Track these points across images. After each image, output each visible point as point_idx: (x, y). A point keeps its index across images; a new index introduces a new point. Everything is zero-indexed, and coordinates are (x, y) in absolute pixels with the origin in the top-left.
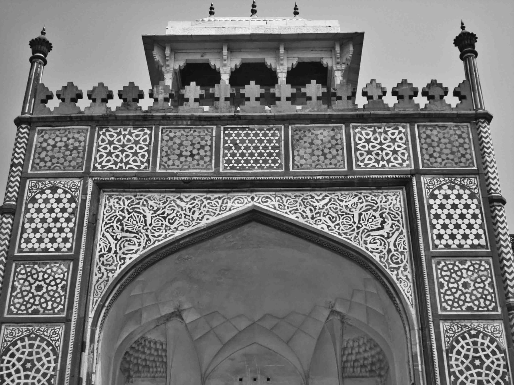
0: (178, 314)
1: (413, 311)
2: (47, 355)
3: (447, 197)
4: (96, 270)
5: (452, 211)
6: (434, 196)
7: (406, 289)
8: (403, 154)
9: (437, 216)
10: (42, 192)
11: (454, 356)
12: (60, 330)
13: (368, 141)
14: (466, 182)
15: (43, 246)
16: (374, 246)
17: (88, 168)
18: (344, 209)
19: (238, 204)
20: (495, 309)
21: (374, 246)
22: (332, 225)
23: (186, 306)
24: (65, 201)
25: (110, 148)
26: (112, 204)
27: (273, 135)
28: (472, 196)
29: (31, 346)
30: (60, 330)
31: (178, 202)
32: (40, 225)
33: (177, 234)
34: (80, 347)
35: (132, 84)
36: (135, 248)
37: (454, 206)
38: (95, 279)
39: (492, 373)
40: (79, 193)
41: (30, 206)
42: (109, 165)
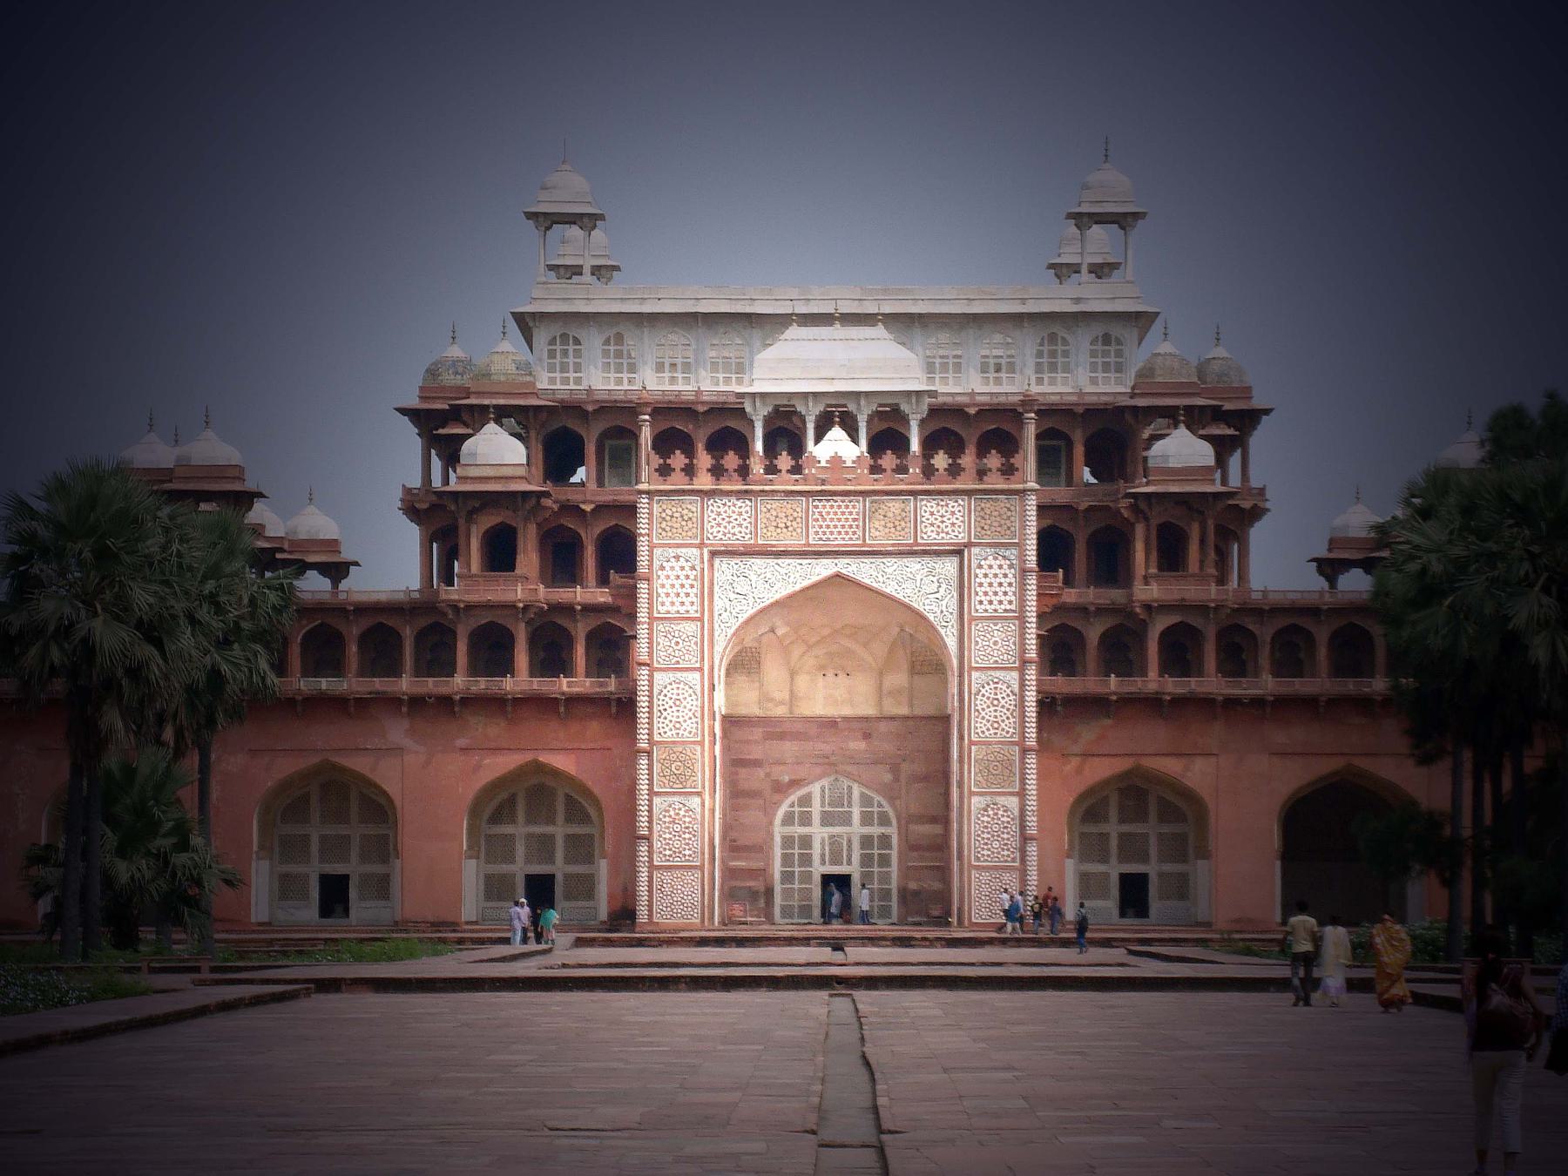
0: (772, 630)
1: (955, 662)
3: (991, 567)
6: (980, 567)
7: (951, 643)
9: (981, 585)
12: (697, 675)
13: (932, 514)
14: (1007, 553)
19: (824, 569)
23: (779, 623)
25: (719, 519)
26: (725, 568)
28: (1011, 567)
33: (777, 596)
34: (712, 687)
37: (996, 576)
40: (697, 562)
42: (720, 536)
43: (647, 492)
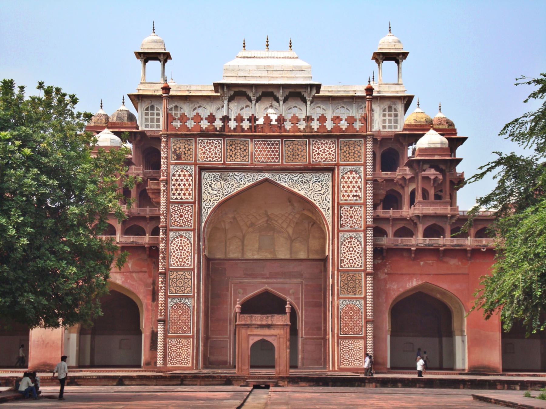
2: (188, 244)
4: (203, 207)
5: (350, 185)
8: (333, 155)
9: (344, 187)
10: (177, 171)
11: (343, 246)
15: (180, 197)
16: (317, 198)
17: (195, 160)
18: (306, 181)
19: (259, 177)
20: (361, 227)
21: (317, 198)
22: (300, 188)
24: (187, 175)
27: (277, 144)
28: (360, 177)
29: (181, 240)
30: (192, 234)
31: (235, 176)
32: (178, 187)
35: (211, 114)
36: (218, 198)
38: (203, 212)
39: (356, 253)
41: (173, 178)
43: (168, 136)
